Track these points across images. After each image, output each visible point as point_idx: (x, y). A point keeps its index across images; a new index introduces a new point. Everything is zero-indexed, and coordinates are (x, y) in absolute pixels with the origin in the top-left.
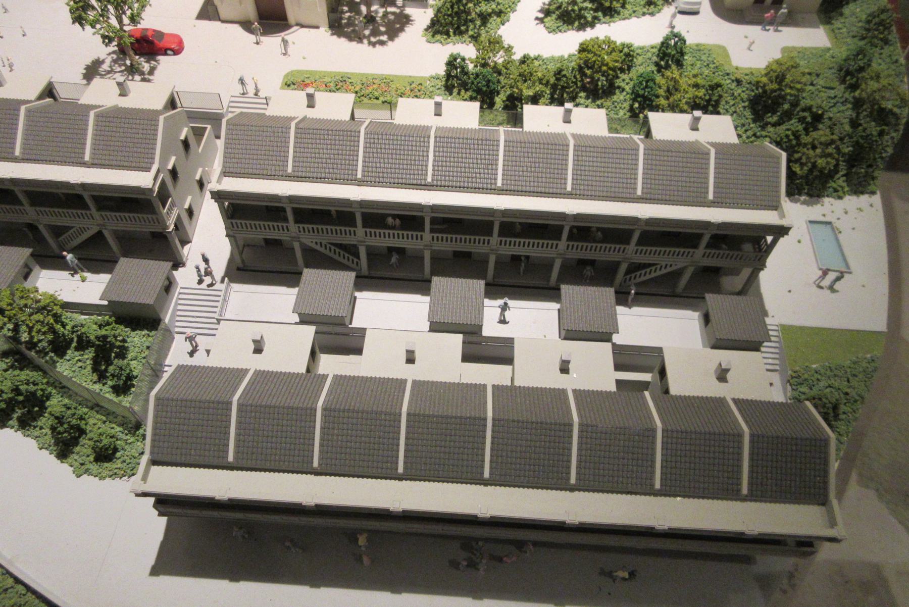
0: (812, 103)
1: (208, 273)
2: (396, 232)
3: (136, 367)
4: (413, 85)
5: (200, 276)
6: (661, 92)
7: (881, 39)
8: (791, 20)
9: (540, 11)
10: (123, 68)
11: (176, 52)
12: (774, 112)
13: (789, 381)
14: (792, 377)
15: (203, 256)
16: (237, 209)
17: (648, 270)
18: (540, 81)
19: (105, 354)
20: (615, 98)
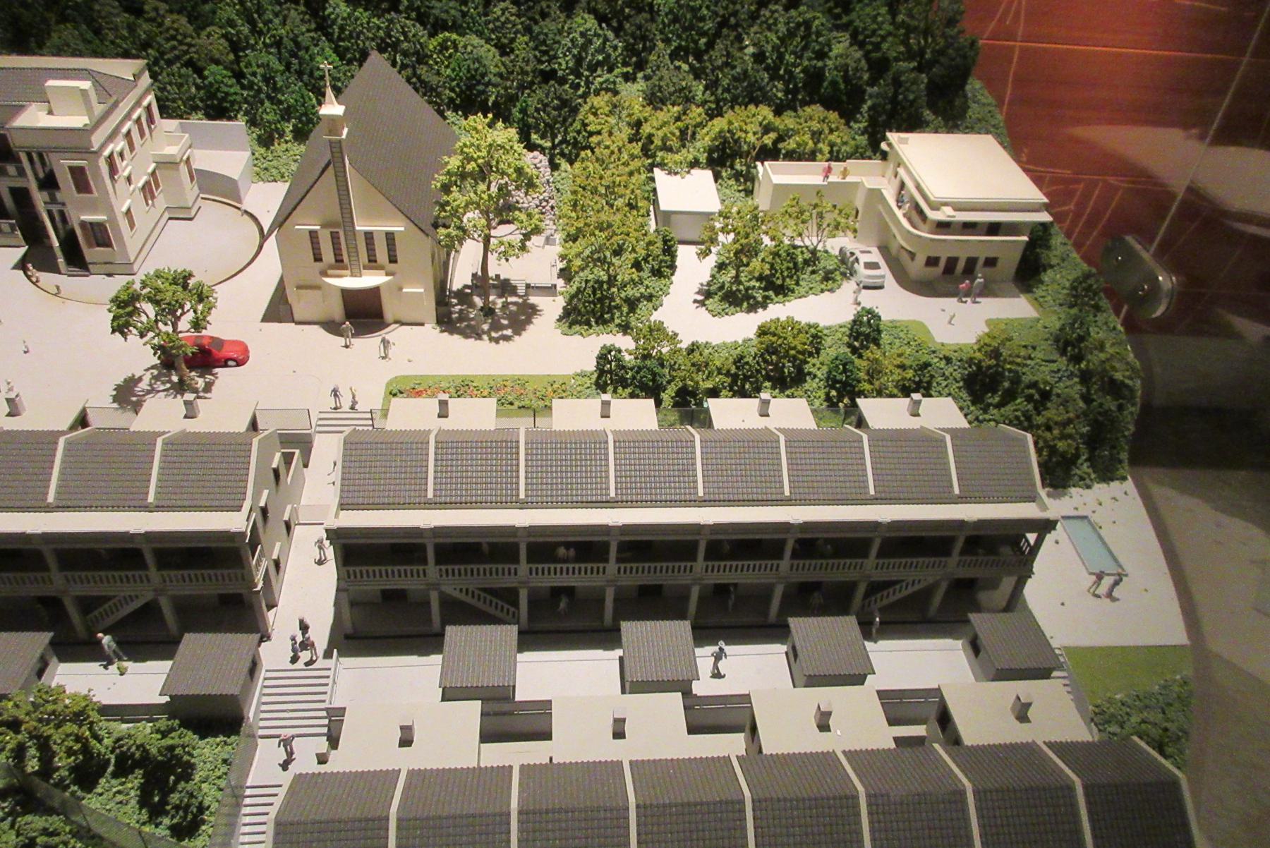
0: (1036, 378)
1: (306, 645)
2: (571, 566)
3: (209, 794)
4: (555, 386)
5: (294, 650)
6: (862, 375)
7: (1093, 306)
8: (987, 291)
9: (698, 293)
10: (168, 385)
11: (239, 363)
12: (994, 392)
13: (1092, 720)
14: (1096, 714)
15: (301, 622)
16: (354, 551)
17: (891, 590)
18: (719, 371)
19: (160, 778)
20: (807, 386)
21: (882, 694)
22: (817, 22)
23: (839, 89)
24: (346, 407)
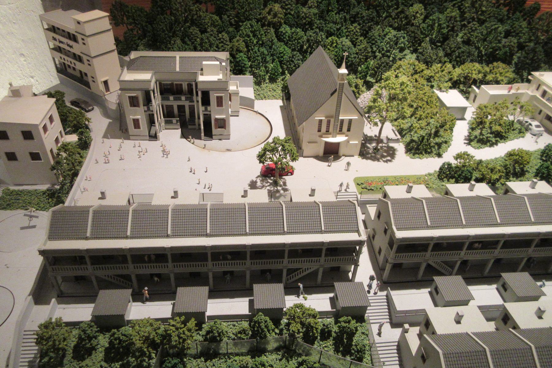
10: (269, 184)
21: (480, 307)
22: (500, 29)
23: (507, 55)
24: (343, 191)
